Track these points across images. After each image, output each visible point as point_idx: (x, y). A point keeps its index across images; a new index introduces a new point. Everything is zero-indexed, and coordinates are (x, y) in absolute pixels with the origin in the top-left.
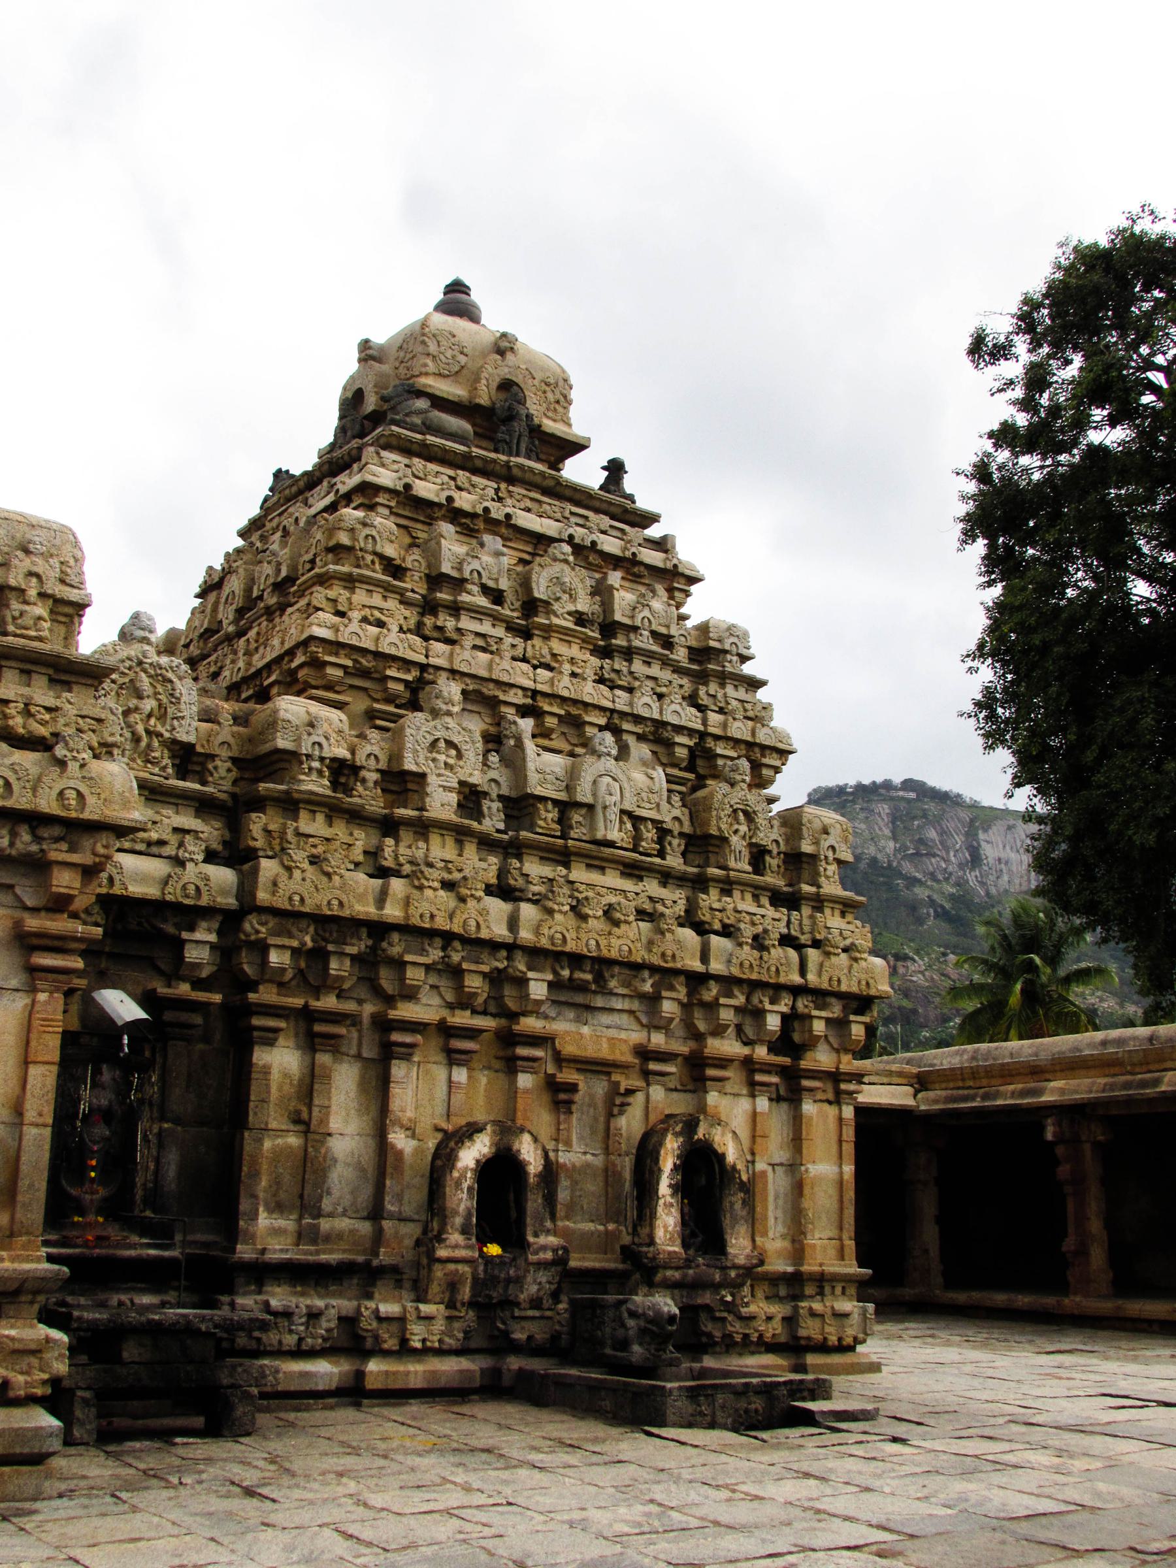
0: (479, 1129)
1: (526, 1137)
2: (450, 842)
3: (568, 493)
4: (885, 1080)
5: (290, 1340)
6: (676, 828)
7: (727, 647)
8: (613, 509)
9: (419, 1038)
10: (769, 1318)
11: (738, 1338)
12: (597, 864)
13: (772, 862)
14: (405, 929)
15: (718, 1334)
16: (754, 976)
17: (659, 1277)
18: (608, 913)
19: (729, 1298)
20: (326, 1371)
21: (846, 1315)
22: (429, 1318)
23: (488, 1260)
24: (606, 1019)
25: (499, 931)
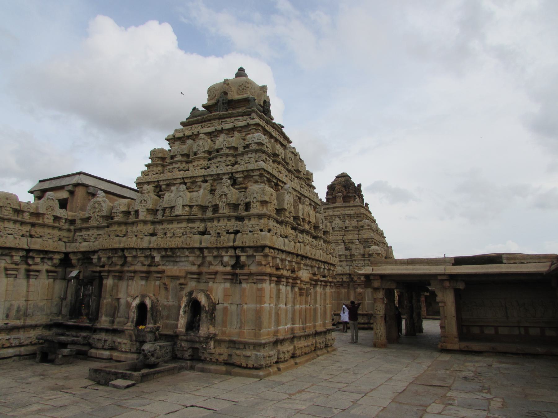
0: (137, 297)
1: (148, 298)
2: (142, 224)
3: (225, 116)
4: (536, 261)
5: (100, 345)
6: (210, 205)
7: (250, 142)
8: (240, 114)
9: (133, 275)
10: (220, 354)
11: (208, 359)
12: (180, 222)
13: (240, 206)
14: (127, 249)
15: (203, 358)
16: (215, 246)
17: (180, 338)
18: (177, 235)
19: (205, 346)
20: (106, 353)
21: (249, 357)
22: (125, 344)
23: (138, 330)
24: (181, 264)
25: (145, 245)
